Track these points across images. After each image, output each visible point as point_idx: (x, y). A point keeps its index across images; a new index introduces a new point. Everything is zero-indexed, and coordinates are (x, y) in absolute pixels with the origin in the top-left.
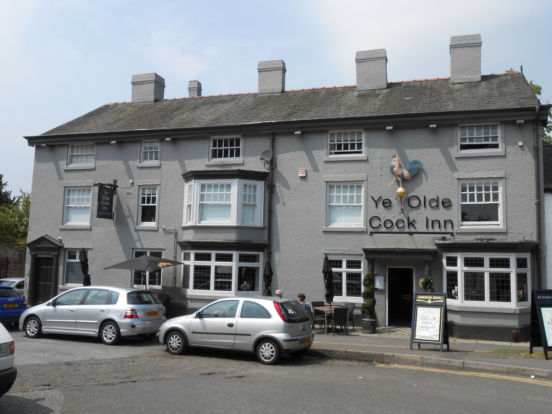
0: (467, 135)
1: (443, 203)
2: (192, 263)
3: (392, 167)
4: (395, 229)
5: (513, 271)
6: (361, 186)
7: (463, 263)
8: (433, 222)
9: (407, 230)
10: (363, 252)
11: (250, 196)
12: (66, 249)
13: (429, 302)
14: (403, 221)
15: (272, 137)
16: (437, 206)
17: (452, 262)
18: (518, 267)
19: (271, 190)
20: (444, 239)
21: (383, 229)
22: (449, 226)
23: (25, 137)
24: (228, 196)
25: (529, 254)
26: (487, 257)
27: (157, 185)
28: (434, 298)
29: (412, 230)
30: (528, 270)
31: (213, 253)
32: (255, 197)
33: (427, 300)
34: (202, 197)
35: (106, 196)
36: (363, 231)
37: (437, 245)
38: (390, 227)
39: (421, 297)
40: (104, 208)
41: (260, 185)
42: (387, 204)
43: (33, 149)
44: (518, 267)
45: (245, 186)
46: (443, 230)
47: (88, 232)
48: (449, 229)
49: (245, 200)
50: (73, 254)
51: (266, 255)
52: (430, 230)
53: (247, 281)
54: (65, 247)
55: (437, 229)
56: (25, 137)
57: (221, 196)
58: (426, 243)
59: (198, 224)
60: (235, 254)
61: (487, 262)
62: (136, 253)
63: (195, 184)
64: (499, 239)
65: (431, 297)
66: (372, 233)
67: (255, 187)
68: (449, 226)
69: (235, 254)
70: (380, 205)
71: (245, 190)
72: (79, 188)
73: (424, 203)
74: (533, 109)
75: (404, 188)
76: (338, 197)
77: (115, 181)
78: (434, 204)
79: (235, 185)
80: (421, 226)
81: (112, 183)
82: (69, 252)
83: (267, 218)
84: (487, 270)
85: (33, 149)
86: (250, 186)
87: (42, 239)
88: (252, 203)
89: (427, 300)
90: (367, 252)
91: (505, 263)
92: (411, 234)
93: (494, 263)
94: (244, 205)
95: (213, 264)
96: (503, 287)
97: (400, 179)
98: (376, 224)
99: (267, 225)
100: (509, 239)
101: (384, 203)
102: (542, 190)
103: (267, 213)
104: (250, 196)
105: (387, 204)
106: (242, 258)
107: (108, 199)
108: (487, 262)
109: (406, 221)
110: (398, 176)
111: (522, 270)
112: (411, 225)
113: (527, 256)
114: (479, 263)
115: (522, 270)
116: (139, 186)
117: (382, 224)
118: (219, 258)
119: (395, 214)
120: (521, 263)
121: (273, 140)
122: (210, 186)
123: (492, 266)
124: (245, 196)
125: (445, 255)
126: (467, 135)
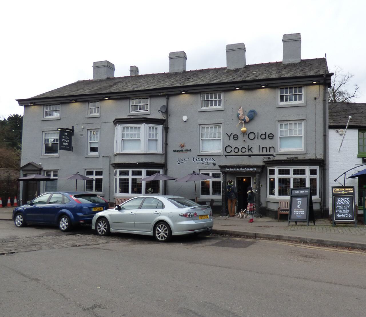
0: (284, 93)
1: (269, 136)
2: (118, 177)
3: (238, 114)
4: (240, 153)
5: (307, 177)
6: (220, 127)
7: (278, 173)
8: (263, 148)
9: (247, 153)
10: (219, 168)
11: (153, 135)
12: (45, 170)
13: (343, 193)
14: (245, 148)
15: (167, 97)
16: (265, 138)
17: (272, 172)
18: (310, 175)
19: (166, 130)
20: (269, 158)
21: (233, 153)
22: (272, 149)
23: (16, 100)
24: (139, 134)
25: (318, 167)
26: (292, 169)
27: (98, 129)
28: (346, 190)
29: (250, 153)
30: (317, 176)
31: (130, 171)
32: (156, 135)
33: (341, 191)
34: (123, 135)
35: (66, 136)
36: (221, 155)
37: (264, 162)
38: (238, 153)
39: (337, 190)
40: (64, 144)
41: (160, 127)
42: (235, 137)
43: (23, 107)
44: (310, 175)
45: (150, 128)
46: (268, 153)
47: (57, 159)
48: (272, 153)
49: (150, 137)
50: (49, 173)
51: (164, 170)
52: (261, 153)
53: (153, 187)
54: (44, 169)
55: (265, 153)
56: (16, 100)
57: (135, 134)
58: (259, 161)
59: (121, 153)
60: (144, 171)
61: (292, 172)
62: (87, 172)
63: (120, 127)
64: (300, 157)
65: (344, 190)
66: (226, 156)
67: (156, 128)
68: (272, 149)
69: (144, 171)
70: (231, 137)
71: (150, 131)
72: (52, 132)
73: (257, 136)
74: (321, 76)
75: (245, 127)
76: (207, 134)
77: (73, 127)
78: (263, 137)
79: (144, 126)
80: (255, 151)
81: (71, 128)
82: (47, 172)
83: (164, 148)
84: (292, 177)
85: (23, 107)
86: (153, 128)
87: (29, 164)
88: (154, 139)
89: (341, 191)
90: (222, 167)
91: (303, 172)
92: (250, 156)
93: (296, 172)
94: (149, 140)
95: (130, 177)
96: (283, 190)
97: (243, 122)
98: (229, 150)
99: (164, 153)
100: (307, 157)
101: (233, 137)
102: (327, 127)
103: (164, 145)
104: (153, 135)
105: (235, 137)
106: (148, 173)
107: (68, 138)
108: (292, 172)
109: (247, 148)
110: (242, 120)
111: (313, 176)
112: (250, 151)
113: (317, 168)
114: (287, 172)
115: (313, 176)
116: (88, 129)
117: (233, 150)
118: (134, 173)
119: (239, 144)
120: (313, 172)
121: (168, 99)
122: (128, 128)
123: (295, 174)
124: (150, 134)
125: (269, 168)
126: (284, 93)
